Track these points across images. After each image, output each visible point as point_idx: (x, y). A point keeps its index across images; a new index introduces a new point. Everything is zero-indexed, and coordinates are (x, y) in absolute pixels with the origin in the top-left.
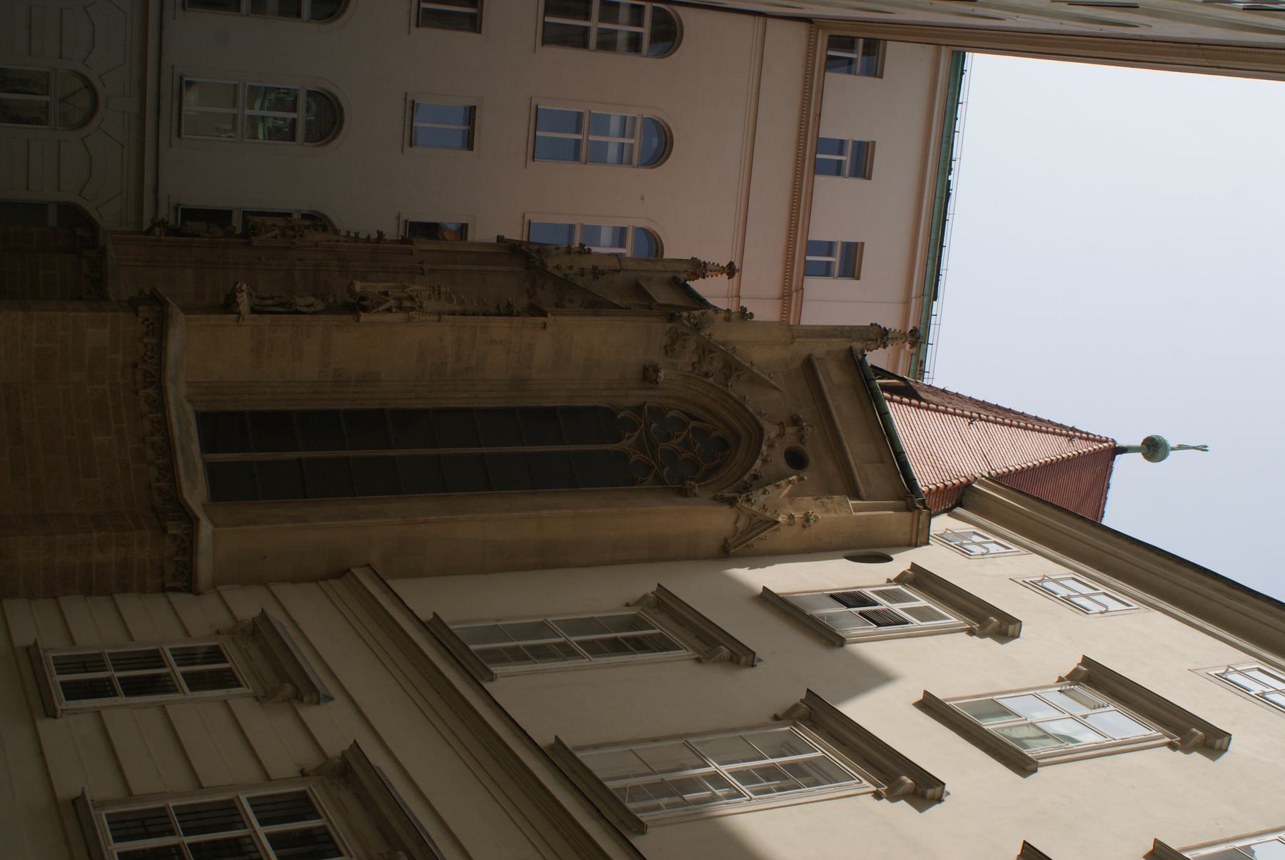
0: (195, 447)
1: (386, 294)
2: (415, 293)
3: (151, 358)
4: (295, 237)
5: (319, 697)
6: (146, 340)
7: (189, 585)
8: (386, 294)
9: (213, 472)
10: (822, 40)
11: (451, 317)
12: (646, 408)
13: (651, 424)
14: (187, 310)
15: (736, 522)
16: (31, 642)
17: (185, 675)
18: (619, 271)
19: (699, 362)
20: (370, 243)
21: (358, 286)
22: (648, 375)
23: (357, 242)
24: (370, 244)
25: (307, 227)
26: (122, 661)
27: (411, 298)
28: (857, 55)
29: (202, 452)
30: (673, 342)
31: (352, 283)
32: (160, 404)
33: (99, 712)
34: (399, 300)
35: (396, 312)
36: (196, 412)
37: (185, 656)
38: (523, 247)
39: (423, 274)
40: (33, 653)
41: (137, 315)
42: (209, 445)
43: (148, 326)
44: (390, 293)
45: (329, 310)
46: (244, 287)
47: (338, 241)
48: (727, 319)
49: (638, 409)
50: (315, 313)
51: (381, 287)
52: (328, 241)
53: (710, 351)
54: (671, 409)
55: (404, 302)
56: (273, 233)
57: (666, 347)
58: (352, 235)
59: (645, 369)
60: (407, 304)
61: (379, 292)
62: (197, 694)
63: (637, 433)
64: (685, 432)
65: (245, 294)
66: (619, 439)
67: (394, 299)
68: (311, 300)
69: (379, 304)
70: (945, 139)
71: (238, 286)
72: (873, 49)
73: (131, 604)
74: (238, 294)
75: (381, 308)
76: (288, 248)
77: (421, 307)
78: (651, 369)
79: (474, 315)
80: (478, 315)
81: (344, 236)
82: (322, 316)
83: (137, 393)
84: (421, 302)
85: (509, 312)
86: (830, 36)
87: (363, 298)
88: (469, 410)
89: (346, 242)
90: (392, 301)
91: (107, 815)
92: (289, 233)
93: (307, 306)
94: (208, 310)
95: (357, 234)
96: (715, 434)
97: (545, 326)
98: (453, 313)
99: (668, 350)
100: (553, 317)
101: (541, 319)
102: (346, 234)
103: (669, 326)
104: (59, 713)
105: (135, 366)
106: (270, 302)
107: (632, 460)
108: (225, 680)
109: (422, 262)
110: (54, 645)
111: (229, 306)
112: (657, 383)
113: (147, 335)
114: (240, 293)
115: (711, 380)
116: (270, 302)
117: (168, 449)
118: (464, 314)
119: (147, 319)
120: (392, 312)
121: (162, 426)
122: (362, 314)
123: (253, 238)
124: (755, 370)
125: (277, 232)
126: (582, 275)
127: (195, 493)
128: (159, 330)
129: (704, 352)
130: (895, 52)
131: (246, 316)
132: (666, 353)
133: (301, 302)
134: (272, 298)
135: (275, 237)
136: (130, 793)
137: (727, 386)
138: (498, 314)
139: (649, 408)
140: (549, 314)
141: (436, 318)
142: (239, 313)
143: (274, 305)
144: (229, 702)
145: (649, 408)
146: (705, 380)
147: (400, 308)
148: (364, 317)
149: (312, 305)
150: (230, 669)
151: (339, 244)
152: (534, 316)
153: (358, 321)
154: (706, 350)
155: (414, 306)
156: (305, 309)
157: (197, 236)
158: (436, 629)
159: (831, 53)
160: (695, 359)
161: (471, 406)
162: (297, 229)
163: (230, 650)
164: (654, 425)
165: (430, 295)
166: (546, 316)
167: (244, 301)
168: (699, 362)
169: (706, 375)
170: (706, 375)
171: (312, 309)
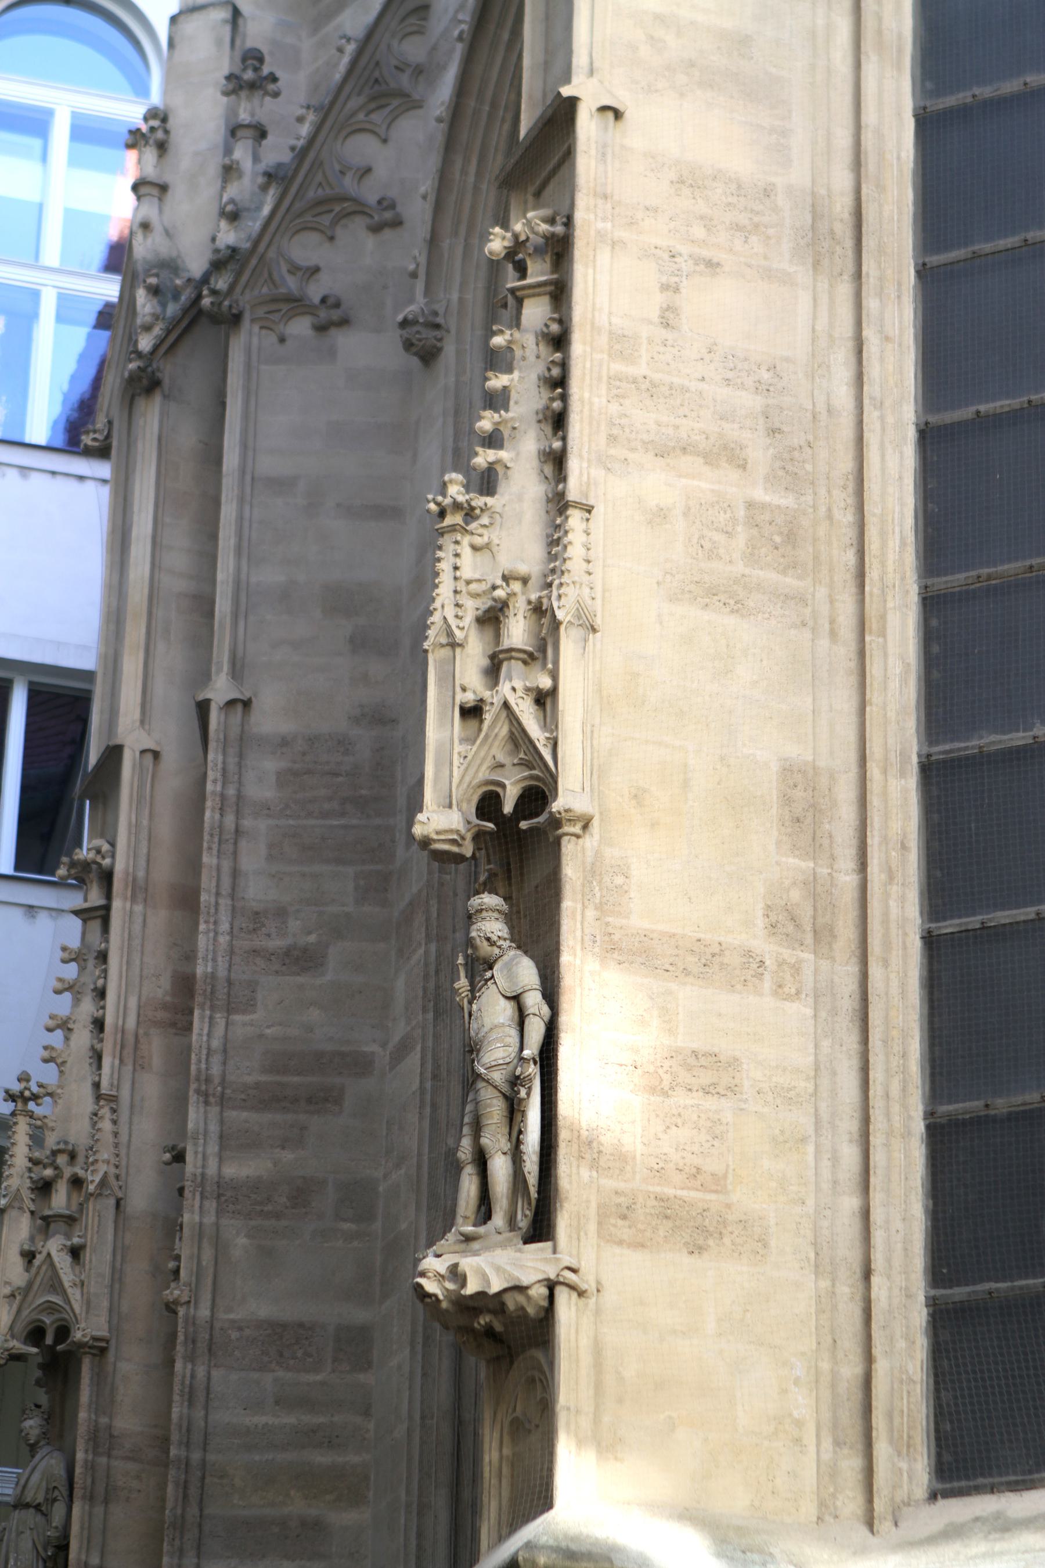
1: (472, 712)
2: (464, 600)
4: (77, 1182)
8: (472, 712)
11: (574, 465)
18: (236, 13)
20: (107, 908)
23: (103, 957)
24: (117, 904)
25: (36, 1139)
34: (493, 671)
35: (555, 676)
36: (933, 1496)
38: (145, 343)
39: (247, 704)
44: (469, 698)
47: (99, 1024)
52: (98, 1057)
55: (506, 644)
56: (63, 1261)
58: (71, 971)
69: (518, 738)
71: (431, 1286)
74: (471, 1288)
76: (118, 1203)
80: (564, 365)
81: (77, 1001)
82: (565, 958)
89: (101, 994)
90: (505, 688)
92: (60, 1200)
95: (76, 957)
100: (575, 80)
102: (67, 996)
106: (500, 1167)
109: (203, 708)
114: (463, 1284)
118: (558, 421)
120: (554, 691)
122: (556, 806)
123: (78, 1335)
125: (55, 1247)
126: (261, 133)
131: (567, 1261)
135: (75, 1253)
140: (566, 91)
141: (575, 519)
143: (516, 1155)
149: (516, 999)
151: (109, 1021)
152: (569, 154)
156: (535, 1031)
157: (63, 1547)
161: (911, 433)
162: (49, 1172)
165: (475, 548)
166: (572, 103)
171: (534, 1000)
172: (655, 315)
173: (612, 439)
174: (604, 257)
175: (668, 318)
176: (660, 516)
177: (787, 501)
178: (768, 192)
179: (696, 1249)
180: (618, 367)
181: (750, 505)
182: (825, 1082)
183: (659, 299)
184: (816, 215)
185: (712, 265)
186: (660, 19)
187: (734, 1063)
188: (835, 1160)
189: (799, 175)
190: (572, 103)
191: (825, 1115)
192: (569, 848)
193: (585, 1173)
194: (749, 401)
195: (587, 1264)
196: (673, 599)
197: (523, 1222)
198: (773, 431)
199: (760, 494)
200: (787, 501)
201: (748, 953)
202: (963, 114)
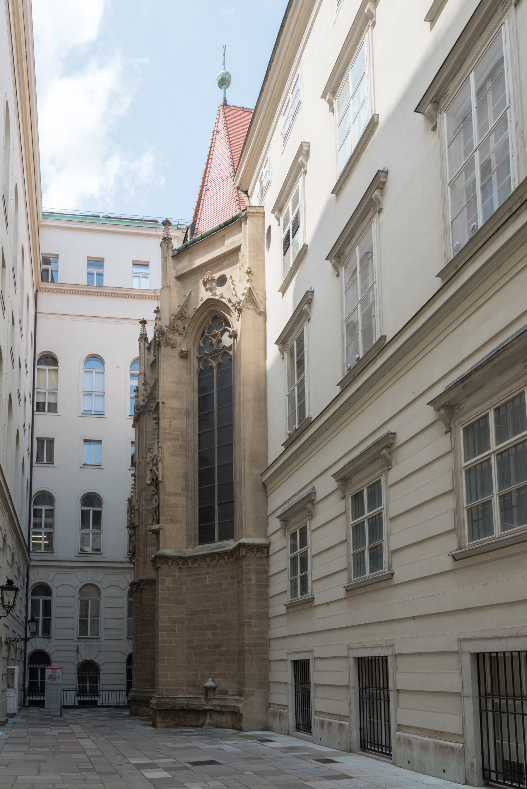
0: (213, 545)
1: (151, 470)
3: (177, 562)
5: (313, 493)
6: (170, 564)
7: (267, 547)
9: (223, 537)
10: (44, 285)
12: (199, 356)
13: (206, 353)
14: (158, 549)
15: (249, 309)
16: (285, 607)
17: (301, 548)
19: (178, 332)
21: (148, 482)
22: (184, 355)
26: (294, 571)
27: (153, 460)
28: (49, 267)
29: (214, 543)
30: (170, 344)
31: (147, 484)
32: (194, 558)
33: (313, 581)
34: (153, 465)
36: (199, 545)
37: (294, 548)
40: (289, 607)
41: (160, 567)
42: (212, 540)
43: (164, 563)
45: (158, 493)
46: (149, 527)
48: (160, 319)
49: (199, 359)
50: (159, 499)
51: (148, 472)
53: (174, 327)
54: (199, 344)
57: (172, 348)
59: (182, 357)
60: (155, 462)
61: (150, 473)
62: (309, 543)
63: (210, 360)
64: (210, 337)
65: (152, 526)
66: (212, 367)
67: (153, 467)
68: (154, 501)
69: (155, 473)
70: (83, 221)
72: (46, 261)
73: (273, 569)
74: (152, 529)
75: (157, 472)
77: (156, 456)
78: (182, 354)
79: (159, 434)
83: (190, 567)
84: (154, 456)
85: (157, 419)
86: (42, 281)
87: (153, 480)
88: (199, 435)
91: (354, 578)
93: (156, 502)
94: (158, 539)
96: (210, 323)
97: (163, 403)
98: (158, 442)
99: (173, 347)
101: (160, 405)
103: (162, 347)
104: (312, 596)
105: (180, 568)
106: (155, 517)
107: (221, 361)
108: (303, 532)
110: (287, 599)
111: (156, 533)
112: (188, 351)
113: (168, 563)
115: (186, 326)
116: (155, 517)
117: (212, 555)
119: (162, 563)
121: (203, 557)
122: (159, 480)
124: (182, 305)
127: (230, 545)
128: (166, 559)
129: (174, 330)
130: (46, 249)
132: (174, 347)
133: (155, 504)
134: (153, 516)
136: (346, 569)
137: (189, 318)
138: (158, 423)
139: (199, 355)
141: (160, 449)
142: (159, 529)
144: (312, 530)
145: (199, 355)
146: (186, 329)
147: (156, 464)
148: (160, 479)
149: (156, 500)
150: (300, 530)
153: (162, 482)
154: (173, 329)
155: (155, 459)
156: (157, 503)
158: (288, 445)
159: (50, 281)
160: (177, 334)
161: (197, 434)
163: (292, 530)
164: (207, 352)
166: (159, 402)
167: (155, 527)
168: (178, 332)
169: (184, 328)
170: (184, 328)
171: (157, 500)
172: (168, 425)
173: (164, 440)
174: (163, 419)
175: (170, 425)
176: (170, 447)
177: (183, 444)
178: (181, 409)
179: (174, 523)
180: (165, 431)
181: (179, 445)
182: (188, 505)
183: (169, 423)
184: (186, 410)
185: (175, 418)
186: (169, 391)
187: (178, 504)
188: (189, 513)
189: (184, 407)
190: (159, 402)
191: (188, 508)
192: (160, 485)
193: (163, 517)
194: (180, 433)
195: (163, 526)
196: (171, 456)
197: (157, 522)
198: (182, 436)
199: (181, 443)
200: (183, 444)
201: (179, 493)
202: (202, 397)
